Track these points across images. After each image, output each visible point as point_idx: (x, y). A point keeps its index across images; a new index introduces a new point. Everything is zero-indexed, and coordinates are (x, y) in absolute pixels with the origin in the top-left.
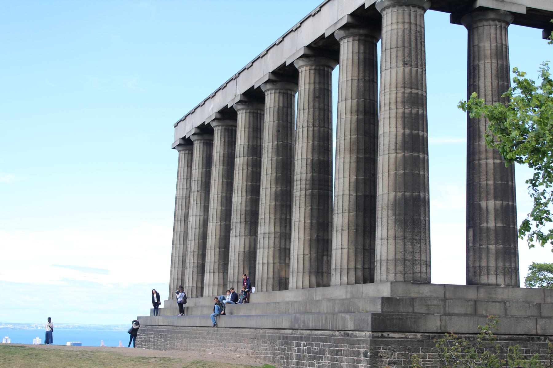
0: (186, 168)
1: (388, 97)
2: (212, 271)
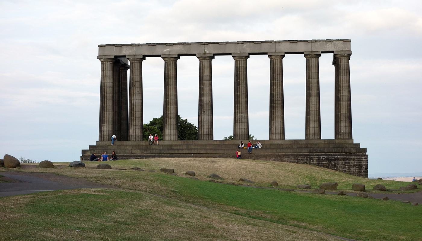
0: (112, 71)
1: (346, 84)
2: (174, 129)
